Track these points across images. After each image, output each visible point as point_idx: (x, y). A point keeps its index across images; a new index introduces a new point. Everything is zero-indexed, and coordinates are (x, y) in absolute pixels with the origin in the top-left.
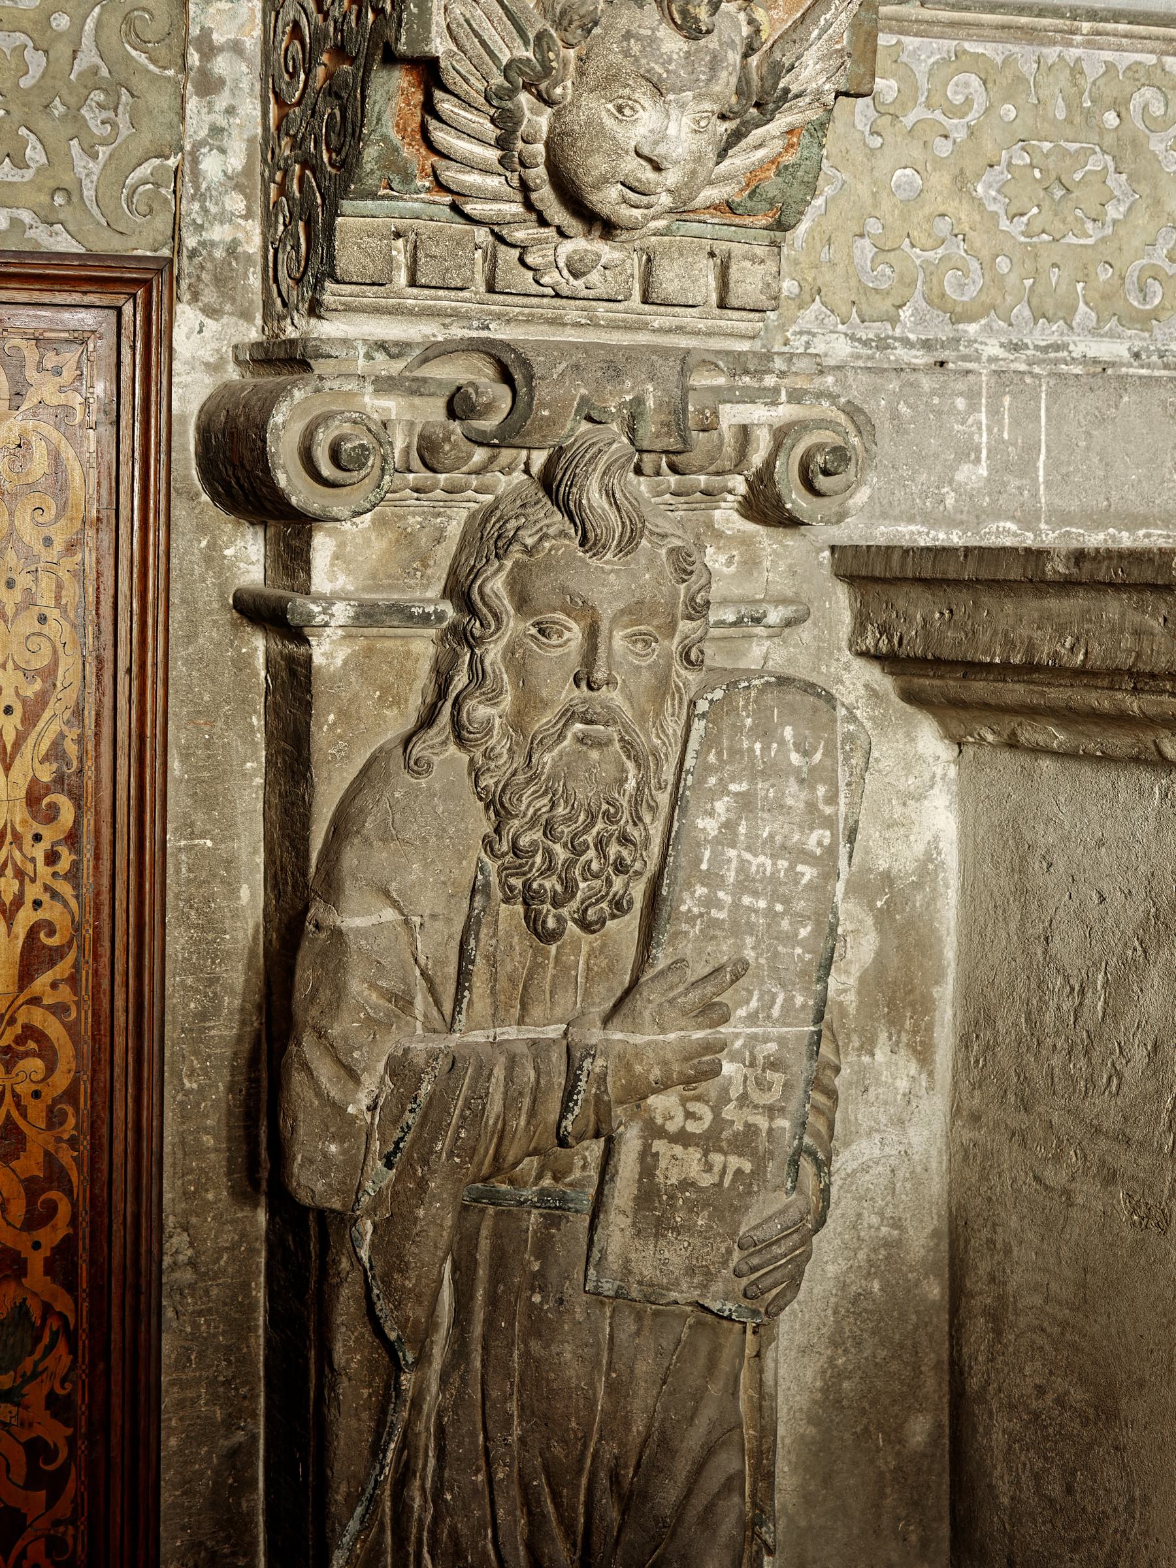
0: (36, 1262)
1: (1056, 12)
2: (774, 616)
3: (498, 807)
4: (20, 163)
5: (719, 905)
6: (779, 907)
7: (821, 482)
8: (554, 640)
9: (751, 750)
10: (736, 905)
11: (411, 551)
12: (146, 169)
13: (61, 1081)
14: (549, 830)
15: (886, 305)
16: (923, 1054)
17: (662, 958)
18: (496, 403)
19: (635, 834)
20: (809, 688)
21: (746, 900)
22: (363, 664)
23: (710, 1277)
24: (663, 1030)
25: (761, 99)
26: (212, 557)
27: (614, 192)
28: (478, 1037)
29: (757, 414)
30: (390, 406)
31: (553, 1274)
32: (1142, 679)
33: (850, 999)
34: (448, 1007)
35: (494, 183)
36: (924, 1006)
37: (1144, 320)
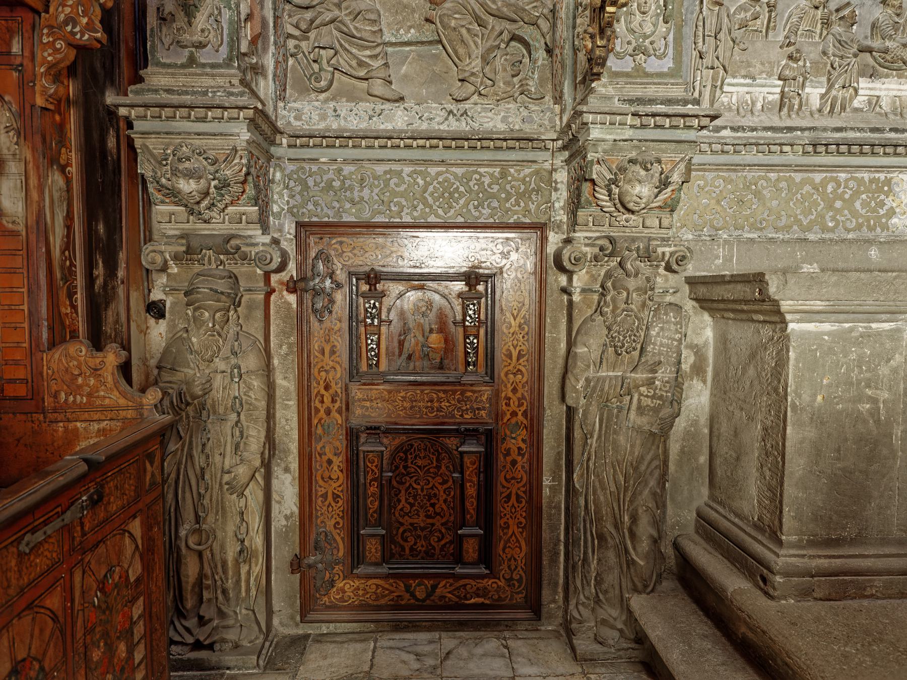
0: (520, 413)
1: (740, 165)
2: (671, 291)
3: (609, 329)
4: (519, 206)
7: (680, 263)
11: (593, 278)
13: (525, 380)
15: (701, 228)
16: (704, 382)
17: (643, 360)
18: (611, 248)
20: (676, 305)
22: (584, 300)
23: (652, 425)
25: (664, 183)
26: (556, 280)
27: (632, 204)
28: (604, 374)
29: (667, 249)
30: (588, 249)
32: (747, 302)
33: (688, 370)
35: (608, 204)
36: (705, 372)
37: (761, 229)
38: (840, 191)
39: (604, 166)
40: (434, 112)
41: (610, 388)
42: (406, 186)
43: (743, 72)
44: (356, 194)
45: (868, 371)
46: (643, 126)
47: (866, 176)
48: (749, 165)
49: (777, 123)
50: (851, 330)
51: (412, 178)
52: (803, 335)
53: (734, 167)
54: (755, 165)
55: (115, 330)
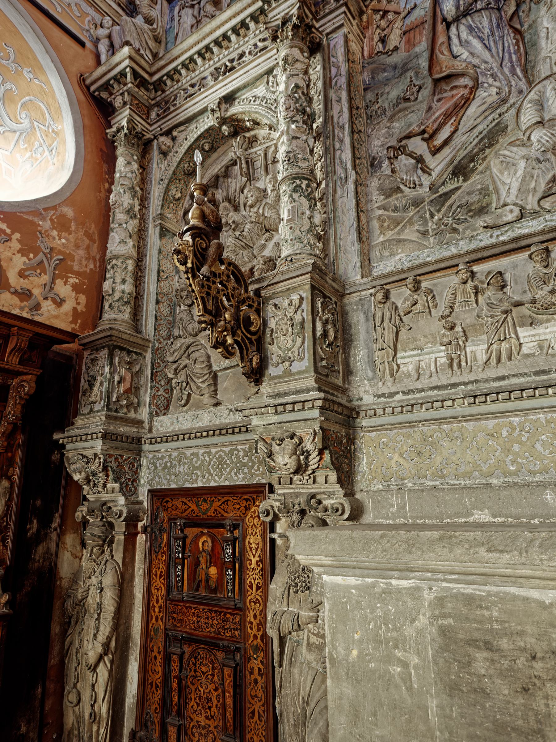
1: (413, 422)
15: (388, 479)
37: (443, 477)
38: (517, 433)
43: (411, 346)
44: (177, 469)
45: (395, 628)
47: (542, 416)
48: (420, 421)
49: (444, 381)
50: (374, 585)
52: (335, 587)
53: (409, 424)
54: (425, 421)
55: (44, 558)
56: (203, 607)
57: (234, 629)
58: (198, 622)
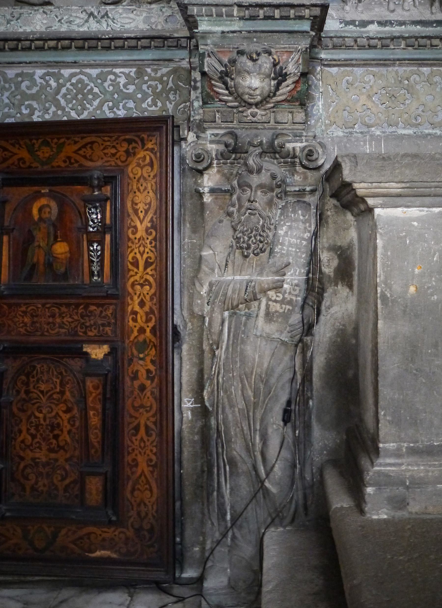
4: (156, 106)
5: (284, 250)
6: (298, 250)
8: (245, 193)
9: (291, 216)
10: (288, 250)
12: (182, 106)
14: (243, 233)
19: (265, 235)
21: (290, 249)
23: (282, 332)
24: (268, 277)
30: (214, 146)
31: (246, 330)
34: (223, 271)
39: (213, 58)
40: (74, 14)
41: (234, 291)
42: (38, 88)
46: (253, 18)
51: (45, 80)
56: (44, 301)
57: (103, 325)
58: (33, 323)
